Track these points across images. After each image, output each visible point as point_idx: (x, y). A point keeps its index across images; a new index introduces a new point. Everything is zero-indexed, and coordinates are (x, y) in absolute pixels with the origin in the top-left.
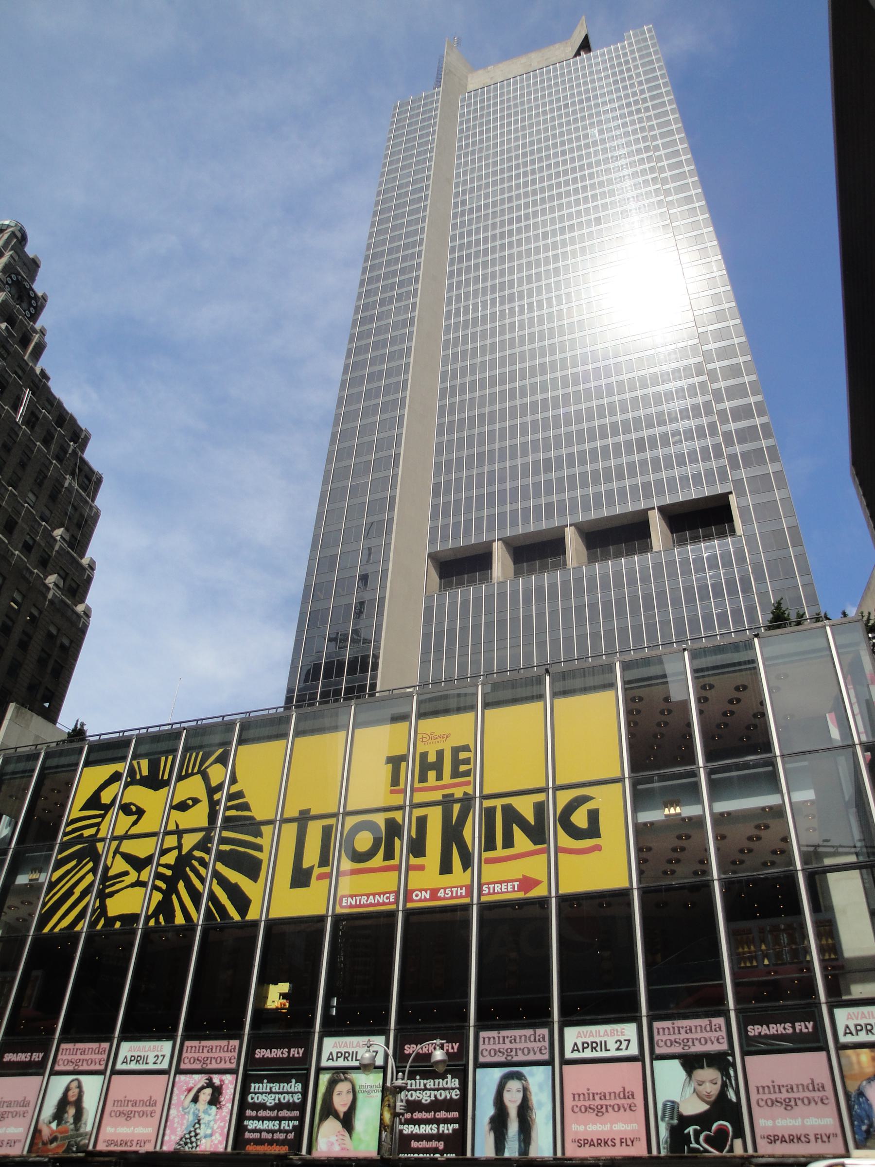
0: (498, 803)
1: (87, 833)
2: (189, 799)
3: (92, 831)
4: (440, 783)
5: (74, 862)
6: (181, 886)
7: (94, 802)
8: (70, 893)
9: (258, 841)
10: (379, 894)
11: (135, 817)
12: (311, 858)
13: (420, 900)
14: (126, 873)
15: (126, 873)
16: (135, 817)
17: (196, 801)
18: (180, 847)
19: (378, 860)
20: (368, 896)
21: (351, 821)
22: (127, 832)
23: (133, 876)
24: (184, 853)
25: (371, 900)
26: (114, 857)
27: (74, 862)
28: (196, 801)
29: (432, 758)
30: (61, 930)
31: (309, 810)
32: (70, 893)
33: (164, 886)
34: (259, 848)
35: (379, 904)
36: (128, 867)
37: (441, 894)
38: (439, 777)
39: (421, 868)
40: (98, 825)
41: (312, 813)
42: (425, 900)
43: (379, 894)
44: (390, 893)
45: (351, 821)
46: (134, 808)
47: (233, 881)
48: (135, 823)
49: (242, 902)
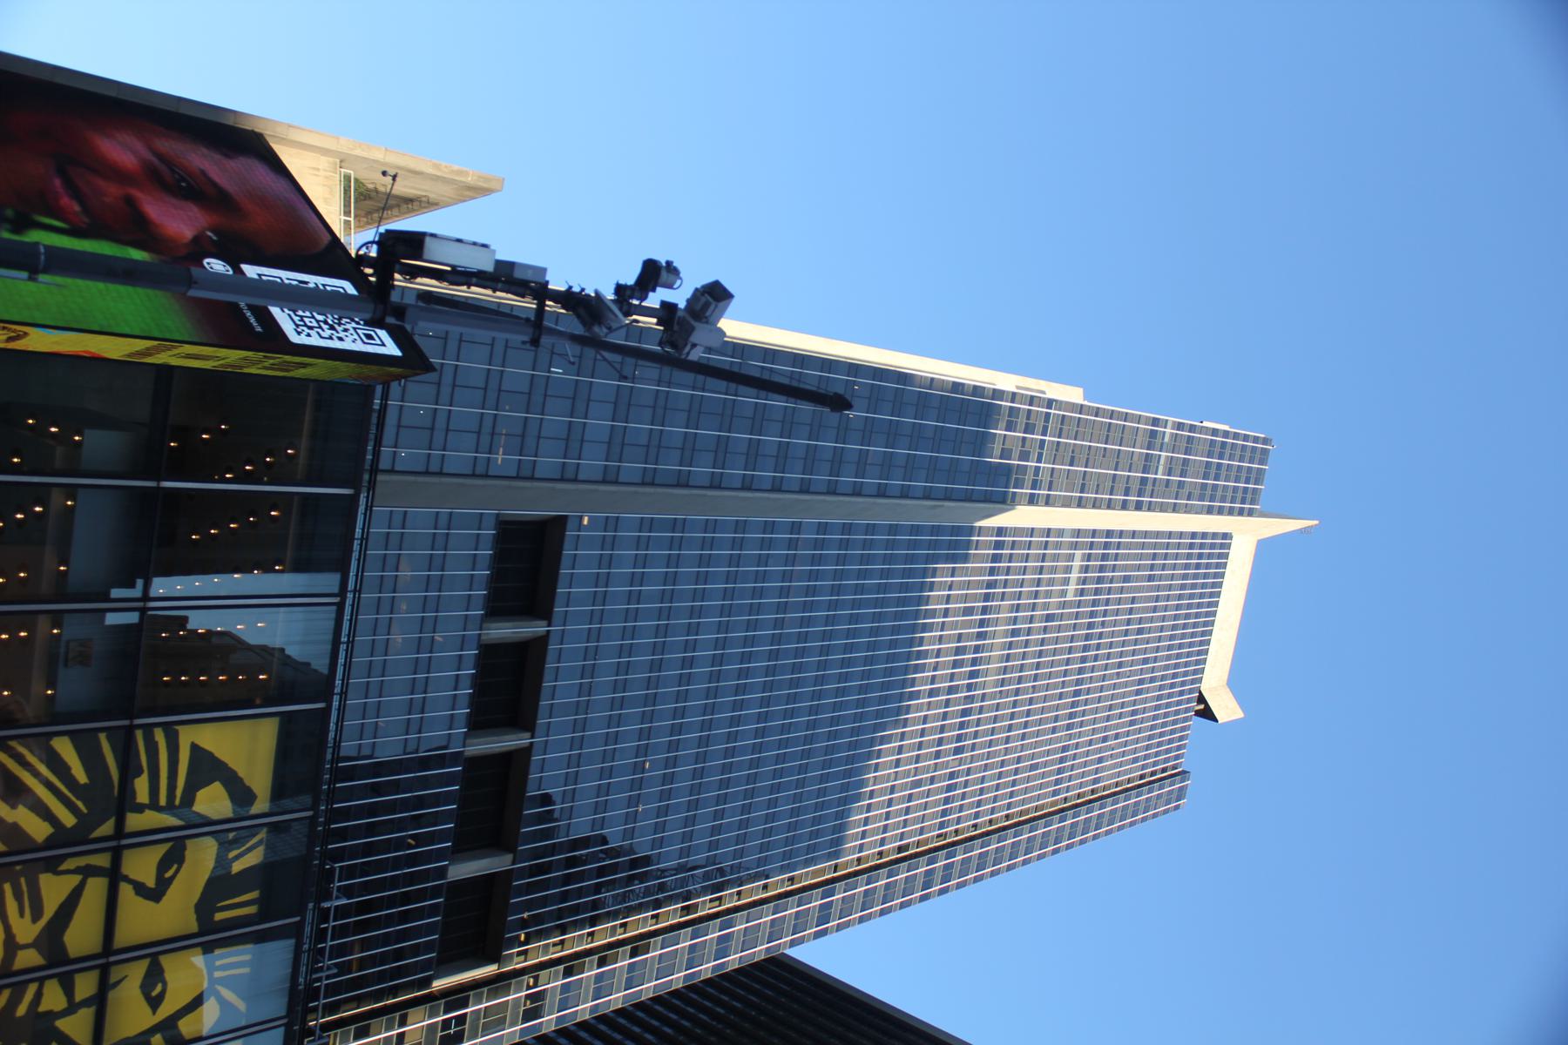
1: (141, 786)
2: (165, 984)
3: (143, 796)
5: (82, 778)
7: (207, 768)
11: (151, 882)
15: (37, 915)
16: (151, 882)
17: (155, 1003)
18: (72, 1008)
22: (127, 879)
23: (26, 930)
27: (82, 778)
28: (155, 1003)
36: (49, 910)
40: (154, 805)
46: (168, 875)
48: (140, 889)
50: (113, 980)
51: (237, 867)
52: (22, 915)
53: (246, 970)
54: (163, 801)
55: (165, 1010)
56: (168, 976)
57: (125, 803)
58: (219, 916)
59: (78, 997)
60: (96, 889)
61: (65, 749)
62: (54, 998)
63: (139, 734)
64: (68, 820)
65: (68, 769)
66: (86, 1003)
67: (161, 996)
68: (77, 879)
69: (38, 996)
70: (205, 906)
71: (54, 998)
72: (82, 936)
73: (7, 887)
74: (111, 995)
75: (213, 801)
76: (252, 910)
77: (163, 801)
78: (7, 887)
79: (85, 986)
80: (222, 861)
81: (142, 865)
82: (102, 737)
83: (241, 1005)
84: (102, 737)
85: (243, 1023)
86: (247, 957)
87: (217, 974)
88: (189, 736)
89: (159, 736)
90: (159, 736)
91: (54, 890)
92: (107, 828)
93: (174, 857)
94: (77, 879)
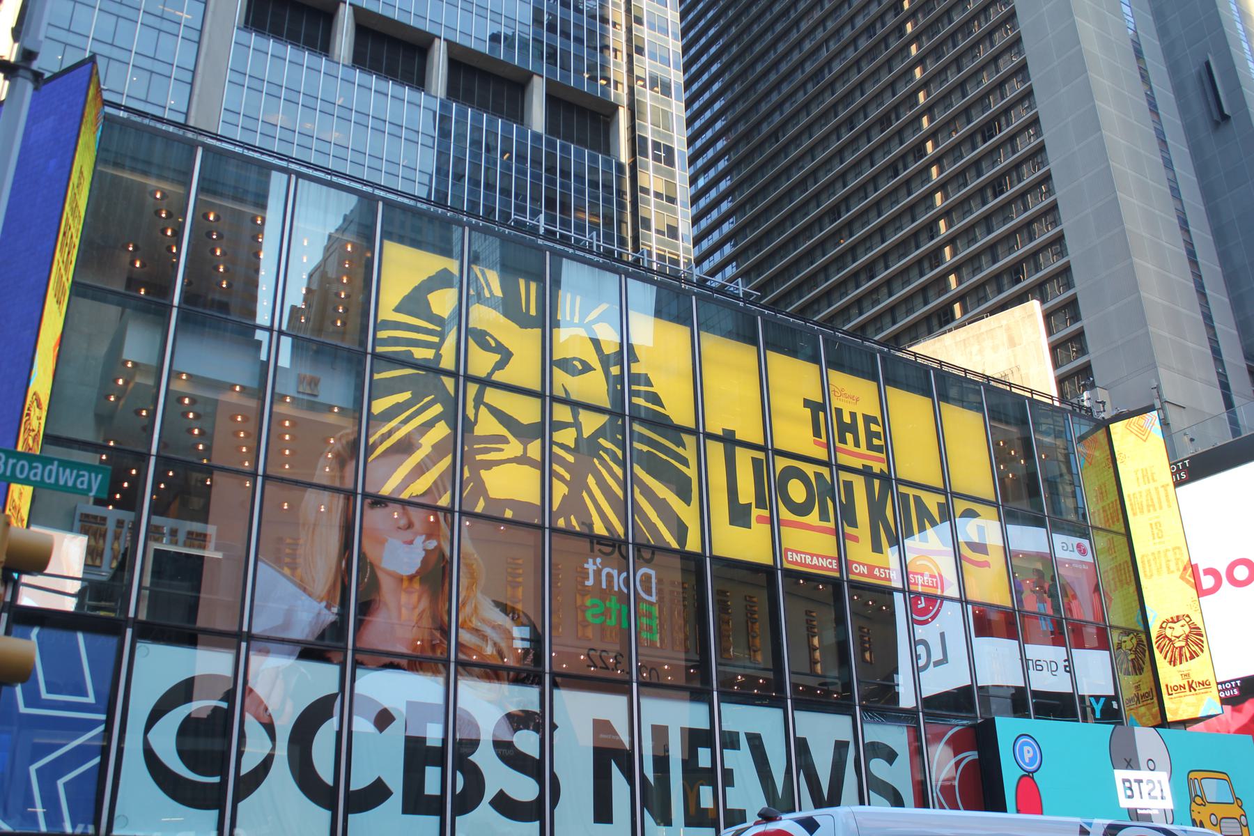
0: (911, 492)
1: (420, 353)
2: (575, 359)
3: (429, 354)
4: (856, 450)
5: (407, 395)
6: (591, 481)
7: (415, 302)
9: (680, 450)
10: (823, 557)
11: (497, 357)
12: (746, 493)
13: (859, 574)
14: (504, 440)
16: (497, 357)
17: (587, 368)
18: (577, 425)
19: (813, 518)
20: (812, 555)
21: (781, 463)
22: (490, 374)
23: (514, 448)
24: (586, 435)
25: (815, 561)
26: (477, 408)
27: (407, 395)
28: (587, 368)
29: (847, 419)
31: (733, 432)
33: (567, 477)
34: (685, 462)
35: (822, 568)
36: (503, 431)
37: (876, 572)
38: (857, 444)
39: (856, 539)
40: (437, 347)
41: (738, 437)
42: (863, 575)
43: (823, 557)
44: (832, 558)
45: (781, 463)
46: (493, 344)
47: (661, 496)
48: (500, 365)
49: (681, 531)
50: (563, 395)
51: (498, 292)
52: (502, 450)
53: (578, 299)
54: (436, 339)
55: (594, 361)
56: (568, 357)
57: (432, 368)
58: (533, 312)
59: (571, 420)
60: (491, 396)
61: (380, 406)
62: (567, 437)
63: (379, 349)
64: (437, 409)
65: (398, 404)
66: (575, 416)
67: (583, 362)
68: (482, 408)
69: (562, 446)
70: (523, 321)
71: (567, 437)
72: (527, 411)
73: (478, 457)
74: (574, 397)
75: (443, 302)
76: (533, 286)
77: (436, 339)
78: (478, 457)
79: (562, 413)
80: (490, 302)
81: (481, 362)
82: (376, 376)
83: (604, 306)
84: (376, 376)
85: (618, 308)
86: (569, 296)
87: (576, 320)
88: (387, 311)
89: (383, 334)
90: (383, 334)
91: (487, 425)
92: (449, 383)
93: (482, 338)
94: (482, 408)
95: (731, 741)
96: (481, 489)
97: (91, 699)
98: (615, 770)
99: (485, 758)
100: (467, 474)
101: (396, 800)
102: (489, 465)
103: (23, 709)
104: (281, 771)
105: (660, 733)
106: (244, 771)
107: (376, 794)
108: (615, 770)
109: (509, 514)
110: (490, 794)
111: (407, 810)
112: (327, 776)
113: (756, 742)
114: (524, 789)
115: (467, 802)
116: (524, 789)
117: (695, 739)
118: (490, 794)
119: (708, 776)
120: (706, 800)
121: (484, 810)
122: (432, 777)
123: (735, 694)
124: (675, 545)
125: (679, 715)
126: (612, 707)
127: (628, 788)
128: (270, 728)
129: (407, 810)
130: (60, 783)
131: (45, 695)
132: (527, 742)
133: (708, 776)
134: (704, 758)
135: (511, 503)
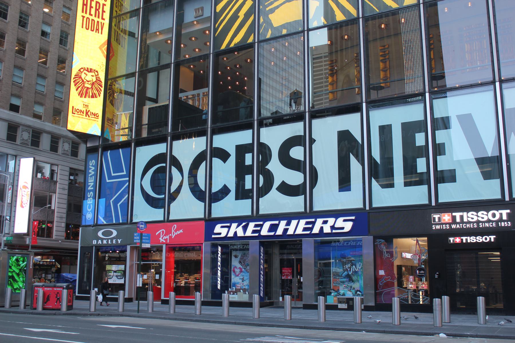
8: (235, 16)
30: (235, 44)
32: (235, 16)
73: (267, 9)
78: (267, 9)
95: (444, 123)
96: (269, 23)
97: (125, 173)
98: (352, 158)
99: (275, 166)
100: (262, 20)
101: (232, 194)
102: (272, 11)
103: (108, 181)
104: (186, 189)
105: (385, 131)
106: (172, 191)
107: (225, 191)
108: (352, 158)
109: (284, 32)
110: (277, 183)
111: (237, 198)
112: (202, 186)
113: (467, 121)
114: (295, 178)
115: (264, 191)
116: (295, 178)
117: (410, 129)
118: (277, 183)
119: (423, 152)
120: (421, 165)
121: (274, 193)
122: (248, 178)
123: (436, 91)
124: (394, 6)
125: (396, 116)
126: (350, 122)
127: (361, 167)
128: (180, 170)
129: (237, 198)
130: (119, 205)
131: (113, 175)
132: (297, 153)
133: (423, 152)
134: (420, 139)
135: (283, 26)
